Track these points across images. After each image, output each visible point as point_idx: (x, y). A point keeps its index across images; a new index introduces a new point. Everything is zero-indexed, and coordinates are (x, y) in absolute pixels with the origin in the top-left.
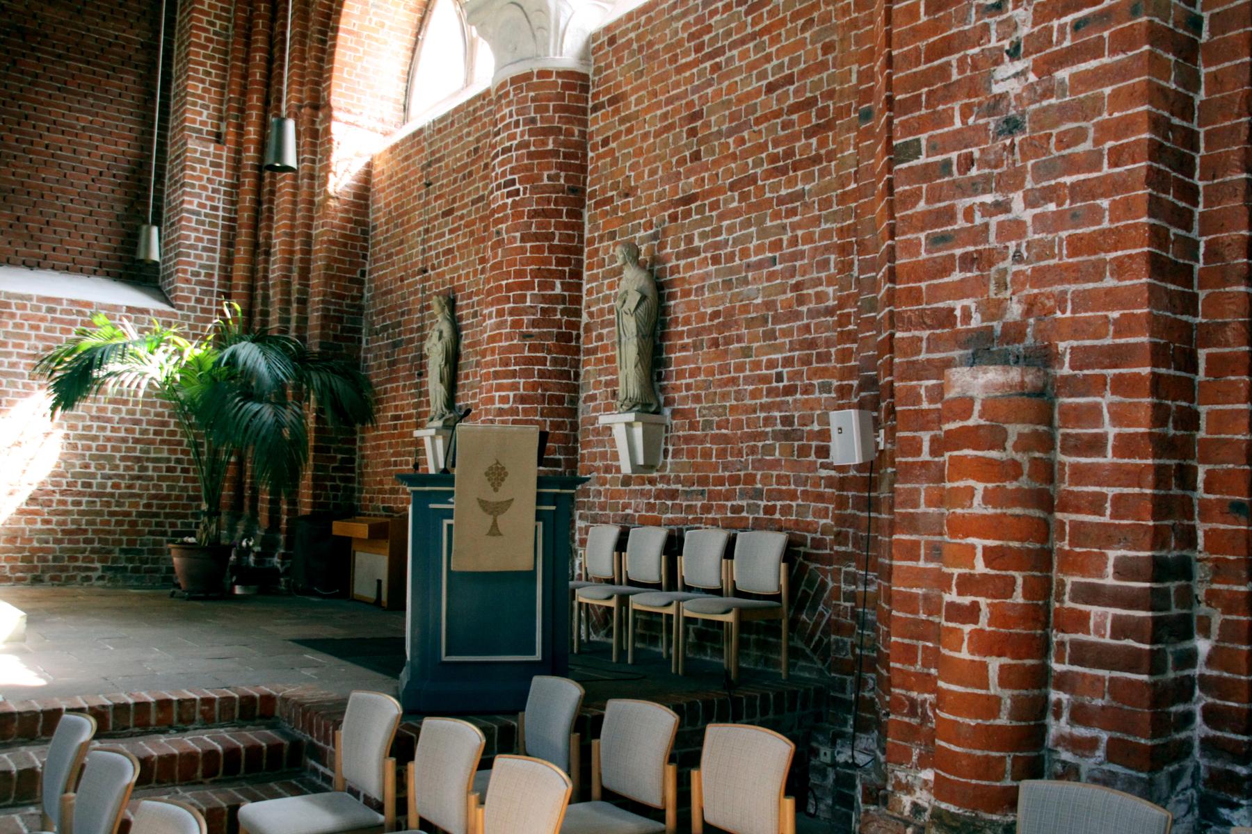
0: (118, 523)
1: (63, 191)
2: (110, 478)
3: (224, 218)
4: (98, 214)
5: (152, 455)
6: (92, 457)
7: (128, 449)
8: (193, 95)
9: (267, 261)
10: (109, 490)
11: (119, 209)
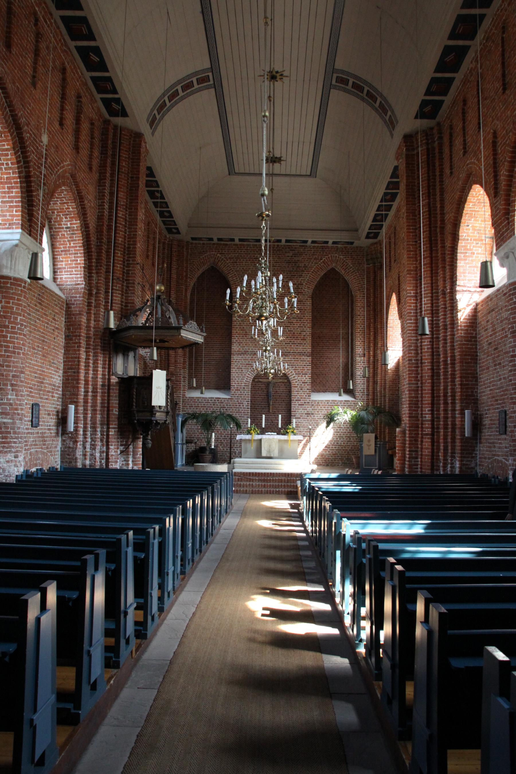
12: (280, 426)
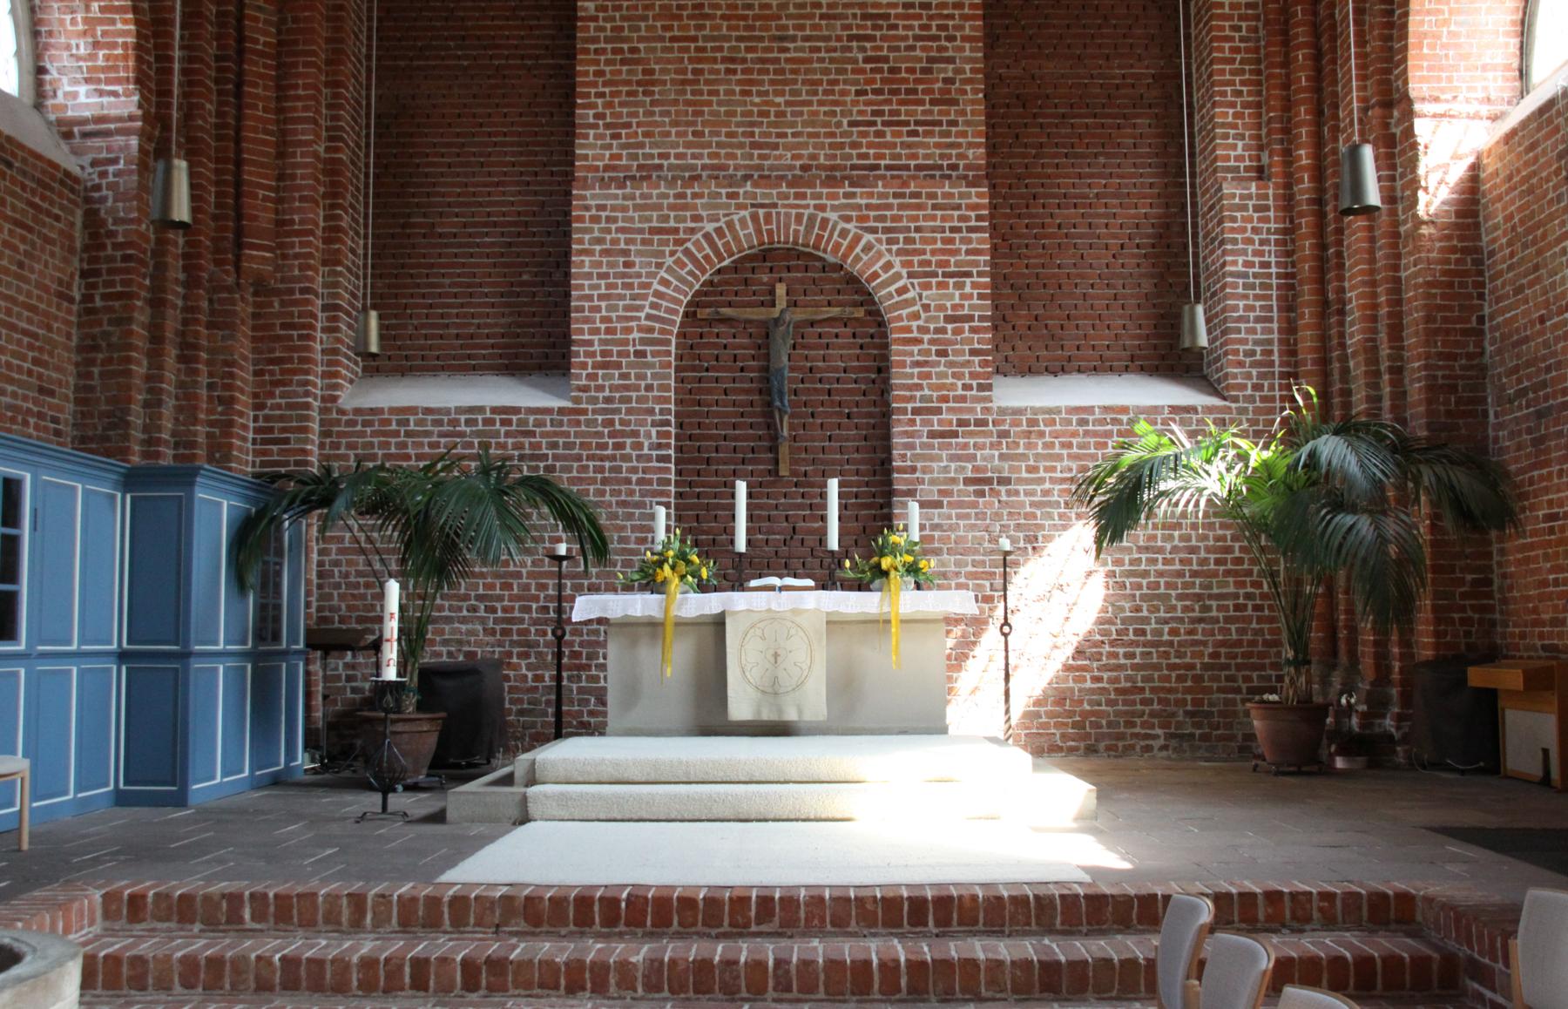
0: (1180, 678)
1: (1082, 276)
2: (1166, 622)
3: (1279, 276)
4: (1124, 297)
5: (1215, 591)
6: (1143, 598)
7: (1186, 585)
8: (1223, 125)
9: (1342, 323)
10: (1166, 637)
11: (1147, 286)
12: (833, 543)
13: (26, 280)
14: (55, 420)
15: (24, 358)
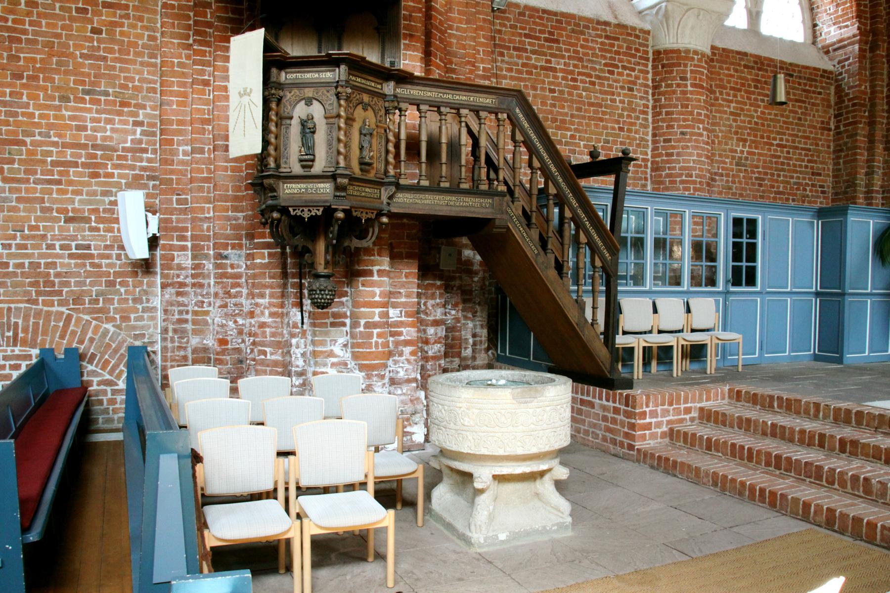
13: (803, 125)
14: (821, 186)
15: (803, 161)
